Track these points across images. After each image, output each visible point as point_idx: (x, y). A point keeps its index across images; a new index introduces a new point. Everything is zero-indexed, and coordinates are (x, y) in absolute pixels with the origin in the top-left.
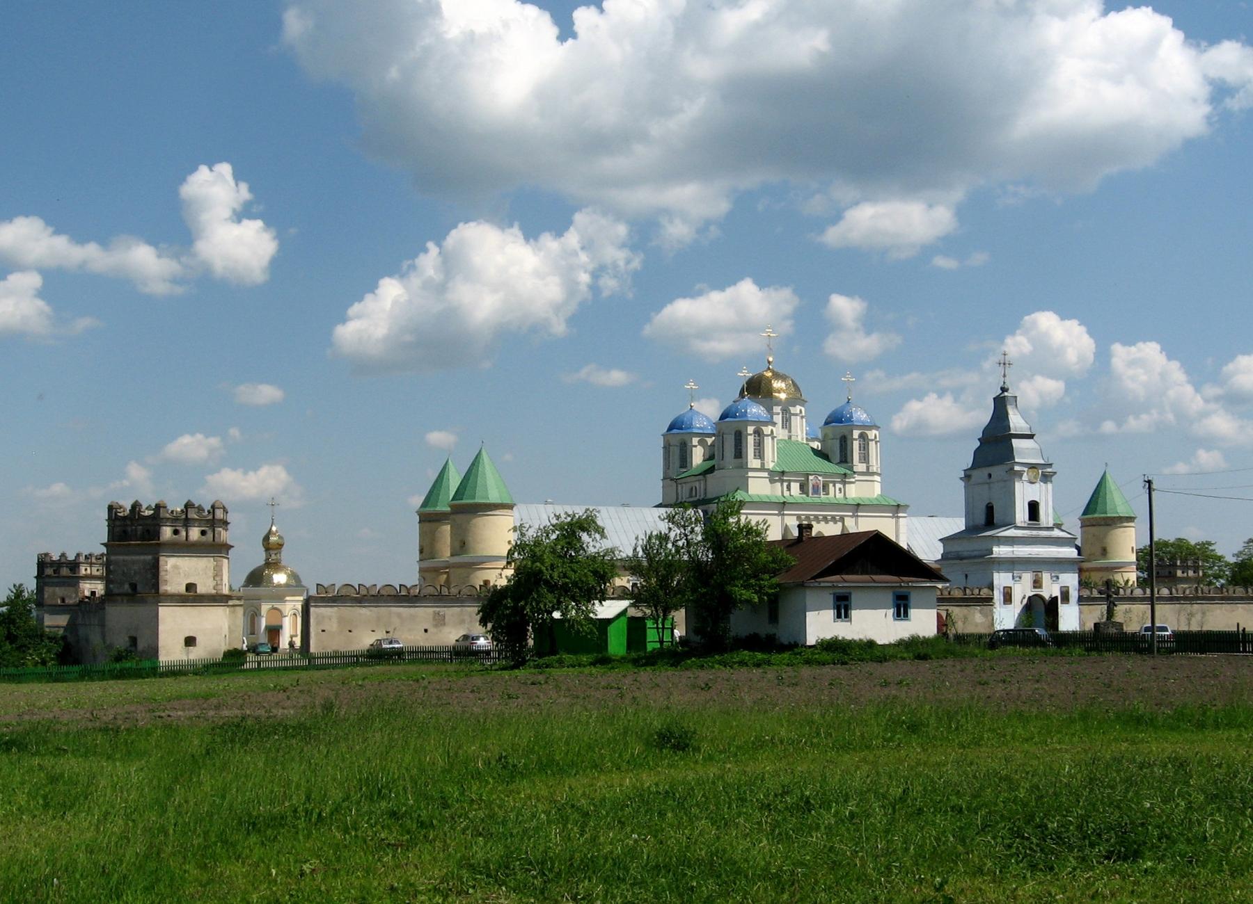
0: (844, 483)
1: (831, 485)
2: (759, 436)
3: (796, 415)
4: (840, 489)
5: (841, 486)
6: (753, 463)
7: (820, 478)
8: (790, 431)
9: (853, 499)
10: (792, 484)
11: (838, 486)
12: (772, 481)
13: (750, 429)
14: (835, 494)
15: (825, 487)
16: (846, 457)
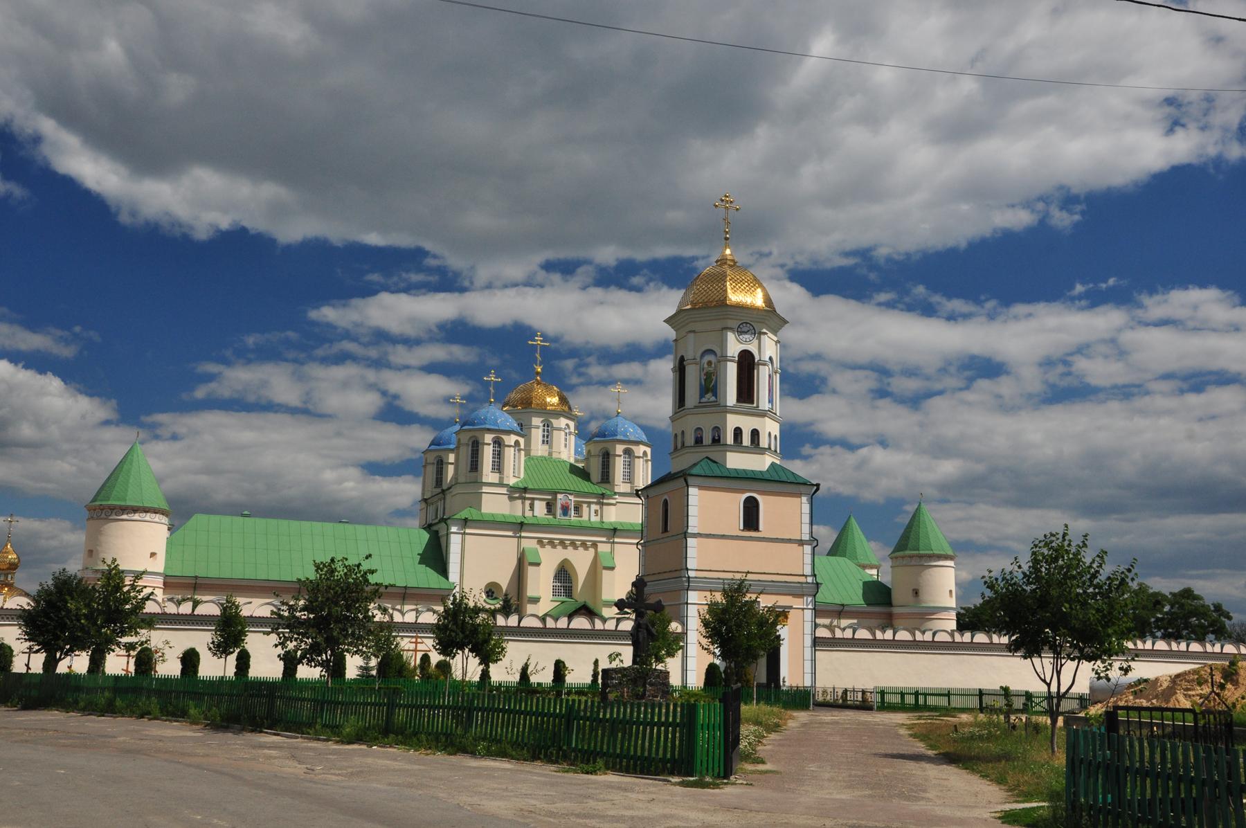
0: (602, 504)
1: (585, 506)
2: (500, 445)
3: (559, 429)
4: (596, 512)
5: (597, 507)
6: (488, 475)
7: (571, 497)
8: (551, 447)
9: (611, 523)
10: (536, 502)
11: (594, 507)
12: (511, 498)
13: (488, 438)
14: (590, 515)
15: (578, 509)
16: (608, 479)
